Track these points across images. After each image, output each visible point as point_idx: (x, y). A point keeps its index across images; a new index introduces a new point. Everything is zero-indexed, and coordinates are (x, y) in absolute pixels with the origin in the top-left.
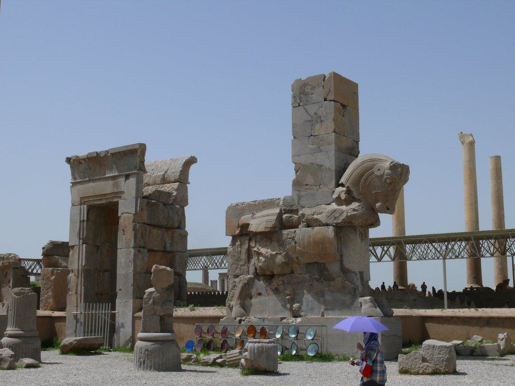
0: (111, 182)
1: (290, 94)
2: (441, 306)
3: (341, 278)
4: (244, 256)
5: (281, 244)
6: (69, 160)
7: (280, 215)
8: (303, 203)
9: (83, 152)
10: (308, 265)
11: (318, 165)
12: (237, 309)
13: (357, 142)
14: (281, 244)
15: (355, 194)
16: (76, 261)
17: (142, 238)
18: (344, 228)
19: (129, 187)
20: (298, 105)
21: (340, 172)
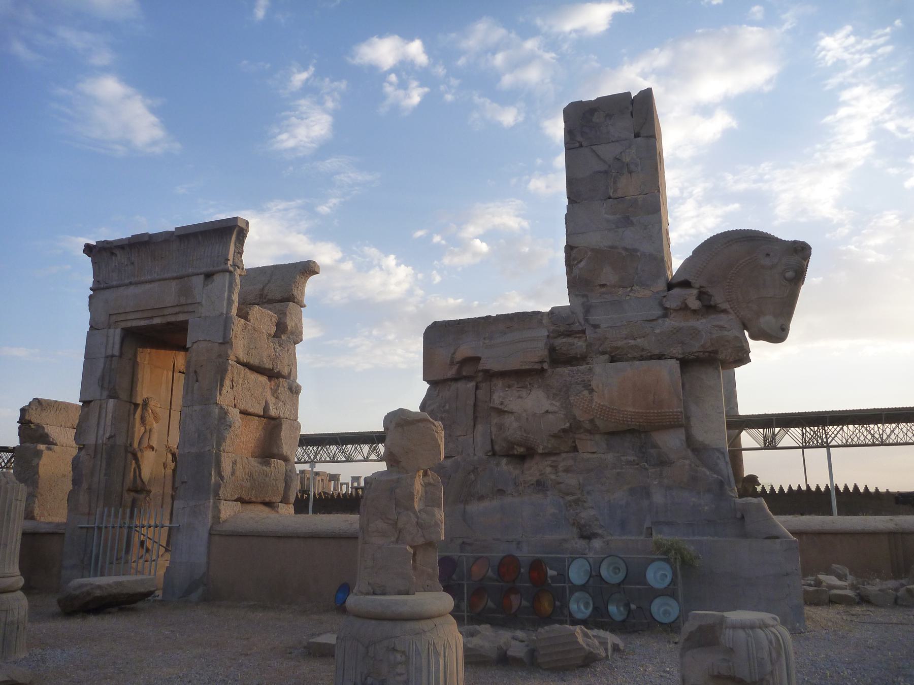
3: (687, 462)
8: (594, 318)
11: (626, 249)
17: (232, 388)
20: (577, 144)
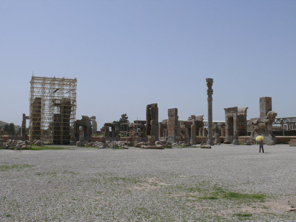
0: (232, 113)
1: (259, 100)
2: (283, 136)
4: (253, 127)
5: (258, 126)
6: (224, 109)
7: (258, 121)
9: (227, 108)
10: (262, 129)
12: (252, 136)
13: (271, 108)
14: (258, 126)
15: (268, 118)
16: (227, 127)
18: (266, 123)
19: (235, 114)
21: (266, 114)
